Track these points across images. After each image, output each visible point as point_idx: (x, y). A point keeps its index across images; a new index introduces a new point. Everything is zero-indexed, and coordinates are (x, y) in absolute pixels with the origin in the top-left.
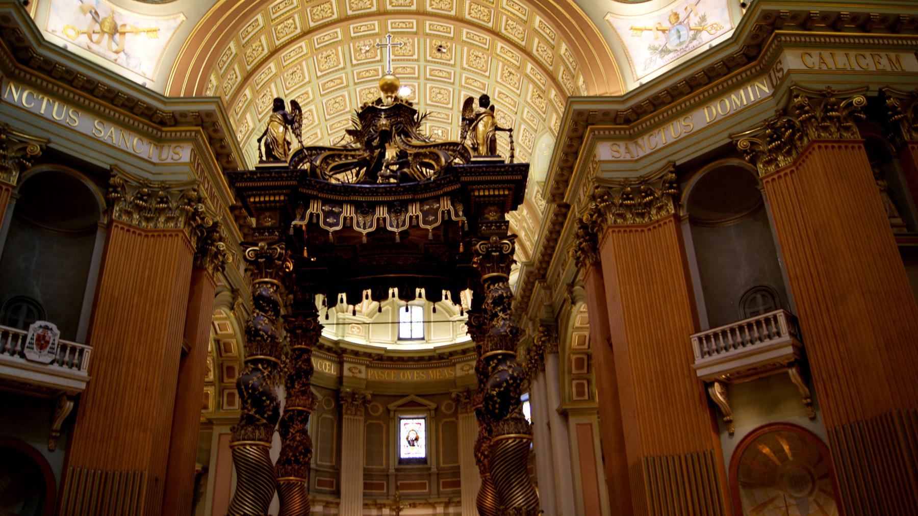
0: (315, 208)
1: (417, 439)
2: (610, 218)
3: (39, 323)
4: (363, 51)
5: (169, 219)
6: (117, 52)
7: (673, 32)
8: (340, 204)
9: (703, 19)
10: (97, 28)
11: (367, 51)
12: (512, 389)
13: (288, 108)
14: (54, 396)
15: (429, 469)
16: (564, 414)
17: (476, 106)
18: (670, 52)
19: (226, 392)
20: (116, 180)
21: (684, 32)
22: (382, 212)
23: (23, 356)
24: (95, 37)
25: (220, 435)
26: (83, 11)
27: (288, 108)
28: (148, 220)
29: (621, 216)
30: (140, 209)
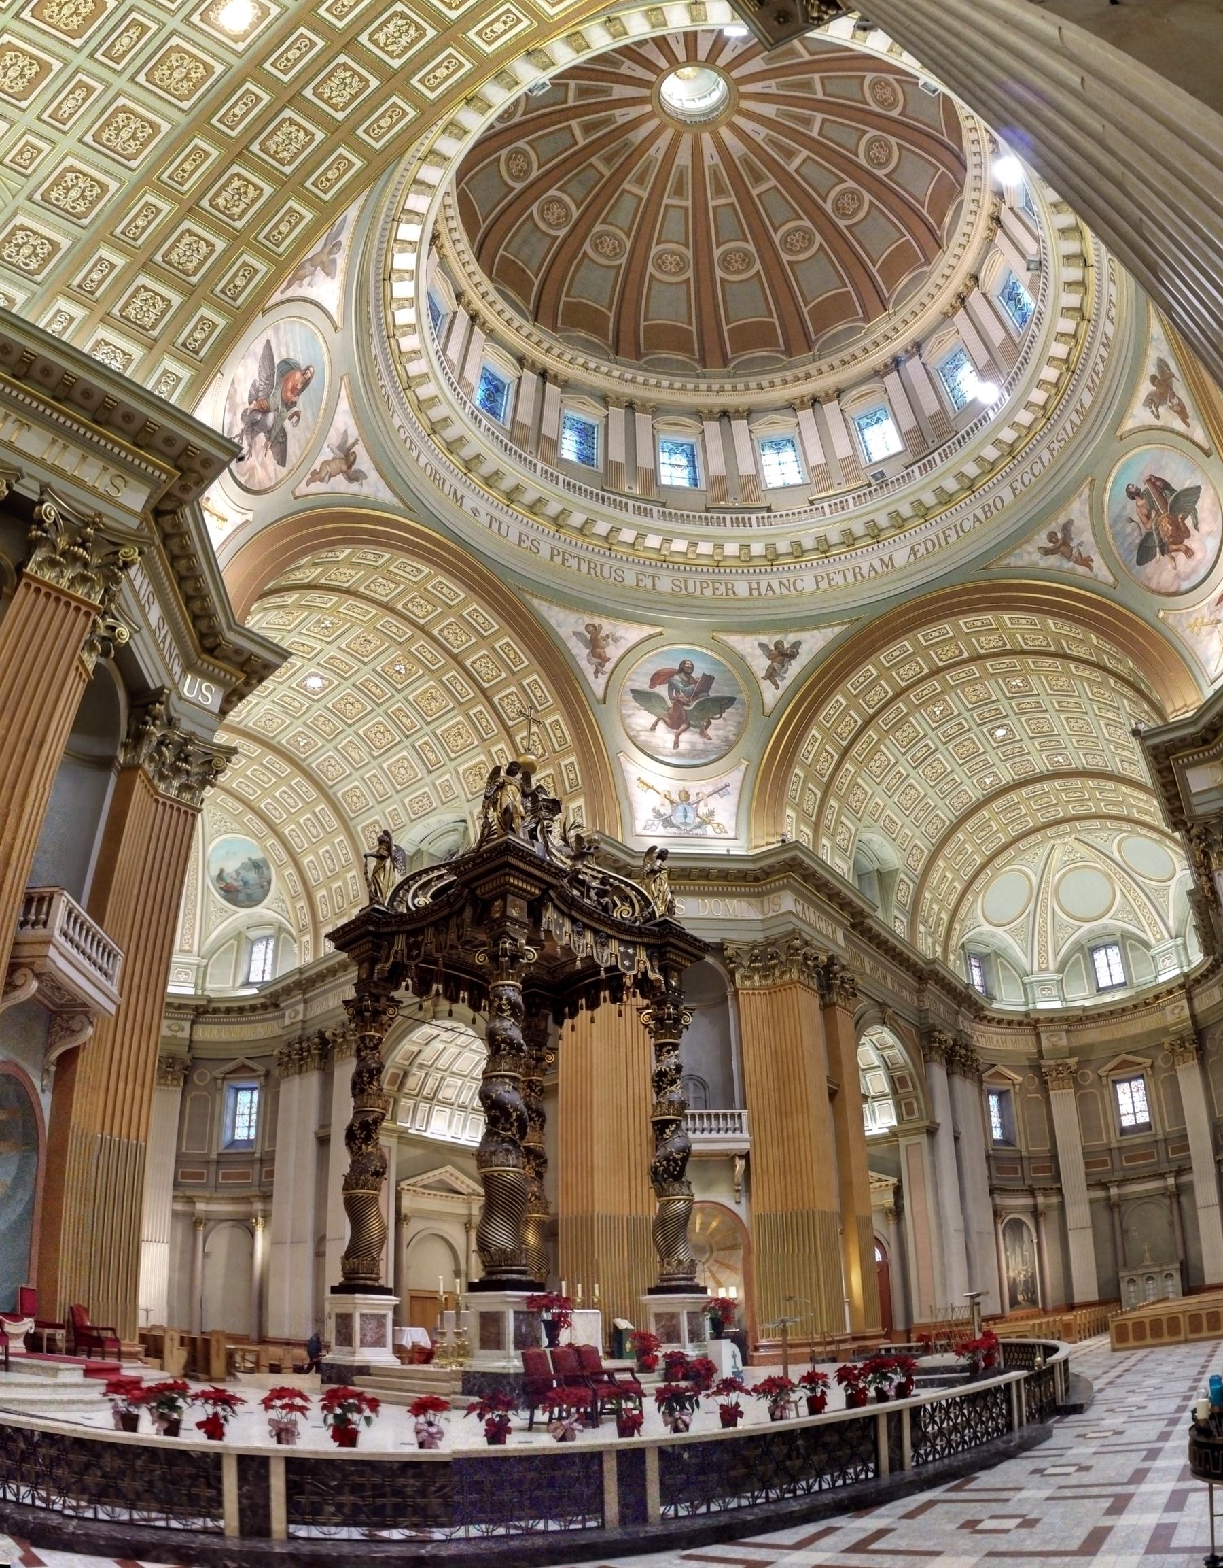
7: (681, 808)
9: (711, 813)
18: (673, 826)
21: (691, 814)
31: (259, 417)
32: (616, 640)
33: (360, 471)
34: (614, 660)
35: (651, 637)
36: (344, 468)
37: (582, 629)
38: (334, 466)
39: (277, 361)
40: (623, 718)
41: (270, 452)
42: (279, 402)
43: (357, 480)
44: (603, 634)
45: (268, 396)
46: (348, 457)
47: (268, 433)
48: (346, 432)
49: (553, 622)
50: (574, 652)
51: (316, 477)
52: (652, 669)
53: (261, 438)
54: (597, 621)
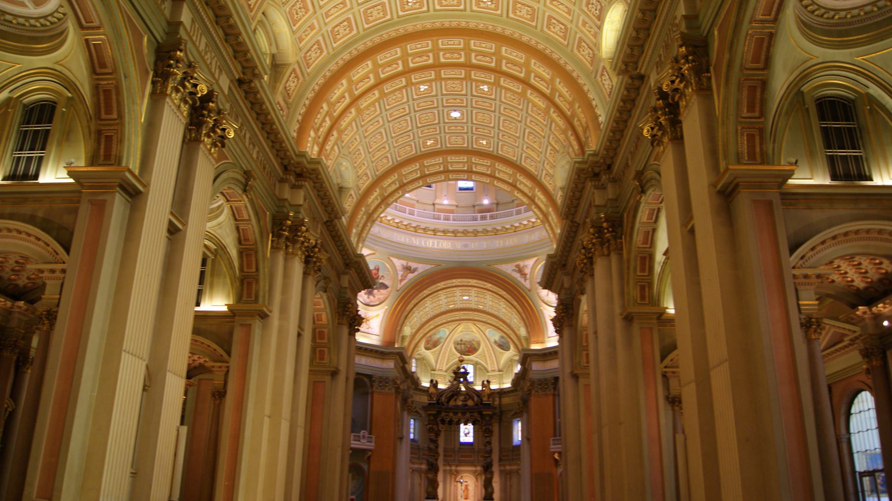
0: (443, 414)
1: (468, 433)
2: (533, 392)
3: (363, 431)
5: (389, 389)
8: (449, 412)
13: (434, 382)
14: (364, 451)
15: (474, 449)
16: (528, 439)
17: (485, 383)
20: (374, 379)
22: (460, 415)
23: (360, 441)
27: (434, 382)
28: (383, 389)
29: (538, 392)
30: (380, 386)
32: (526, 266)
35: (536, 261)
37: (514, 268)
38: (405, 274)
40: (538, 294)
41: (382, 291)
46: (408, 269)
48: (403, 265)
49: (504, 270)
50: (515, 276)
51: (401, 281)
54: (517, 263)
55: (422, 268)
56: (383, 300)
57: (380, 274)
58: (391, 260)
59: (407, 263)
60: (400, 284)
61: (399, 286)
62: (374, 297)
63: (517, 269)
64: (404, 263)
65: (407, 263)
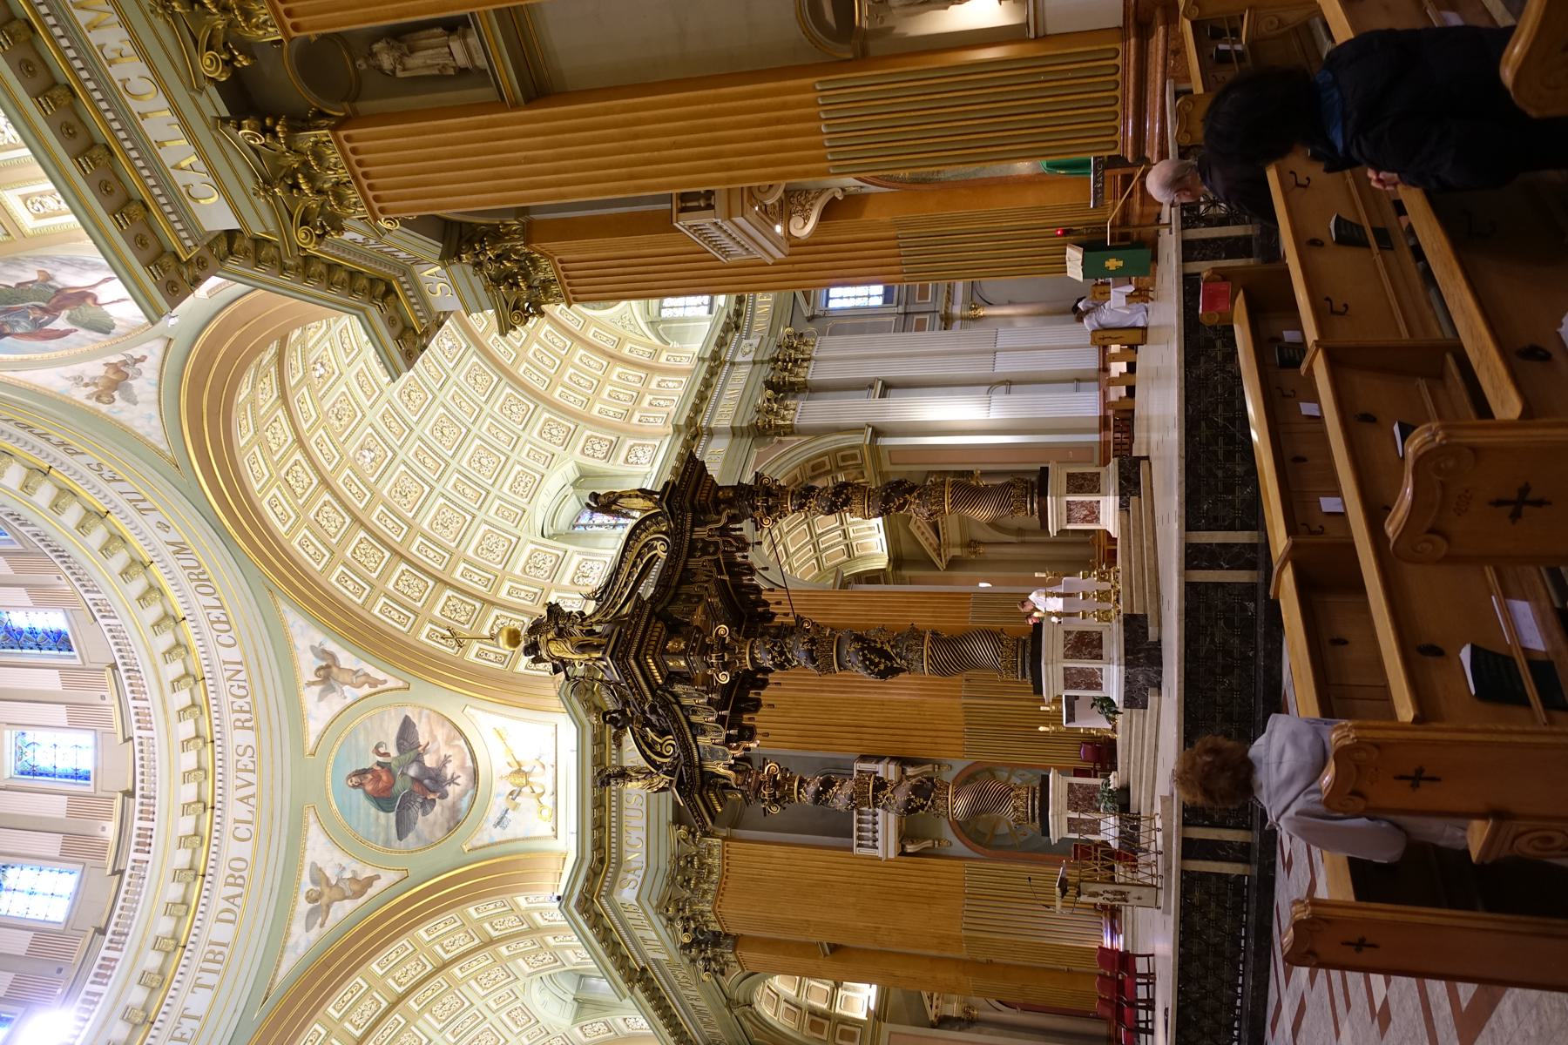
4: (373, 455)
6: (544, 767)
10: (526, 790)
11: (369, 450)
12: (876, 670)
19: (842, 464)
24: (538, 790)
25: (892, 464)
26: (516, 807)
31: (426, 782)
33: (316, 655)
34: (101, 361)
36: (334, 669)
37: (119, 402)
38: (347, 678)
39: (393, 816)
41: (422, 742)
42: (399, 778)
43: (324, 651)
44: (92, 389)
45: (411, 792)
46: (328, 674)
47: (418, 759)
48: (321, 697)
49: (156, 422)
51: (374, 683)
52: (52, 343)
53: (429, 761)
54: (92, 403)
55: (306, 637)
56: (448, 724)
57: (370, 761)
58: (320, 738)
59: (310, 684)
60: (385, 682)
61: (392, 683)
62: (446, 760)
63: (116, 394)
64: (309, 695)
65: (310, 684)
